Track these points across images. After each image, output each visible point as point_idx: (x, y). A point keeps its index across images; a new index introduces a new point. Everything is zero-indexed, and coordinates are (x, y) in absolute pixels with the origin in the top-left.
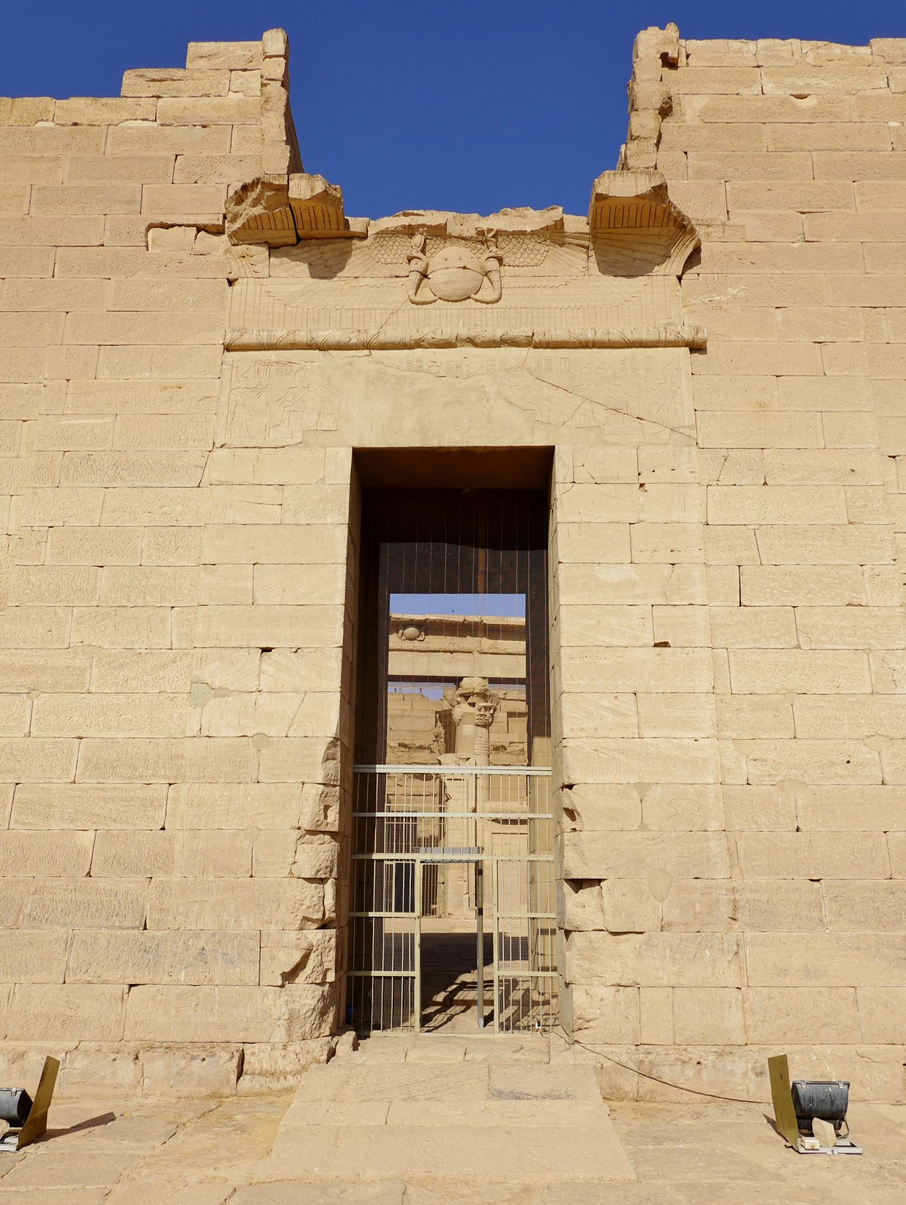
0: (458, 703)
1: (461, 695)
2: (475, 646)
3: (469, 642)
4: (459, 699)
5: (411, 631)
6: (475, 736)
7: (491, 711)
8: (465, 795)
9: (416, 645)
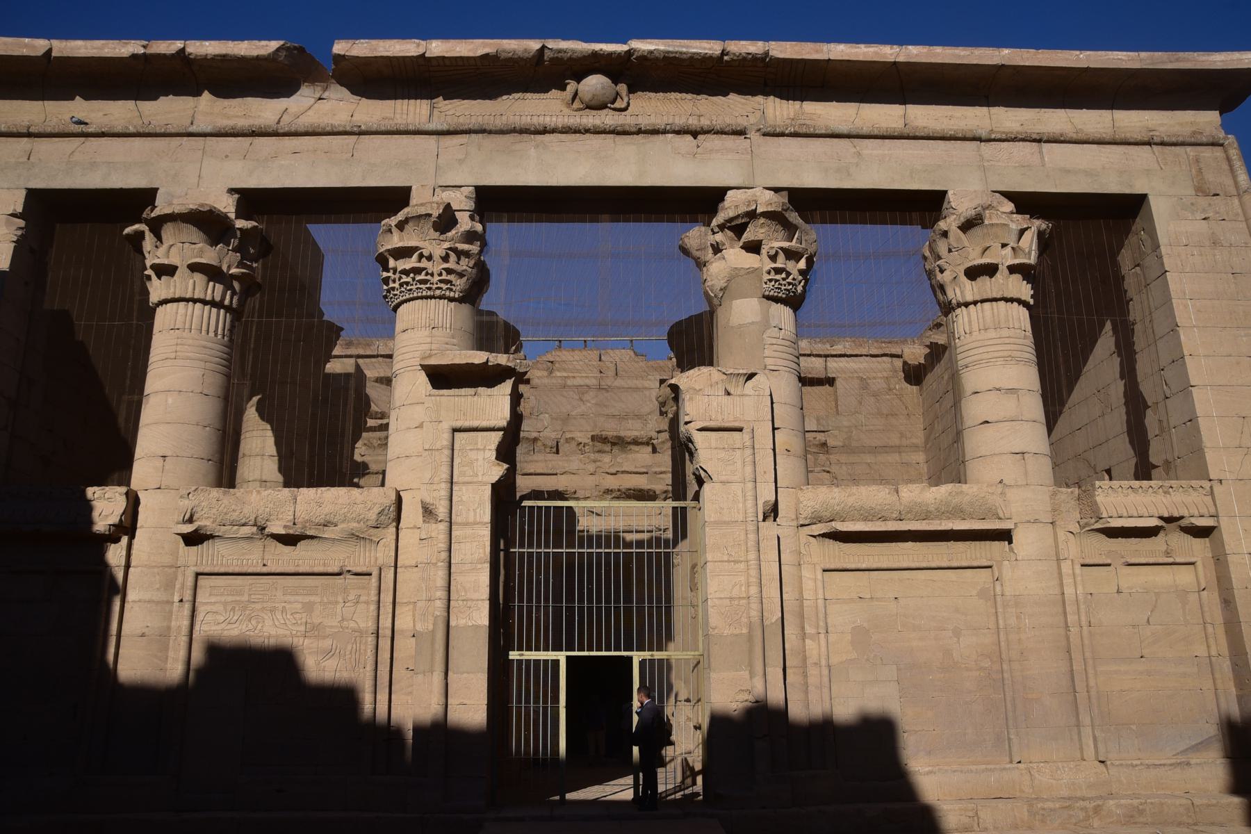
0: (717, 249)
1: (722, 227)
2: (752, 120)
3: (735, 108)
4: (719, 237)
5: (595, 83)
6: (765, 323)
7: (802, 264)
8: (749, 469)
9: (606, 118)
